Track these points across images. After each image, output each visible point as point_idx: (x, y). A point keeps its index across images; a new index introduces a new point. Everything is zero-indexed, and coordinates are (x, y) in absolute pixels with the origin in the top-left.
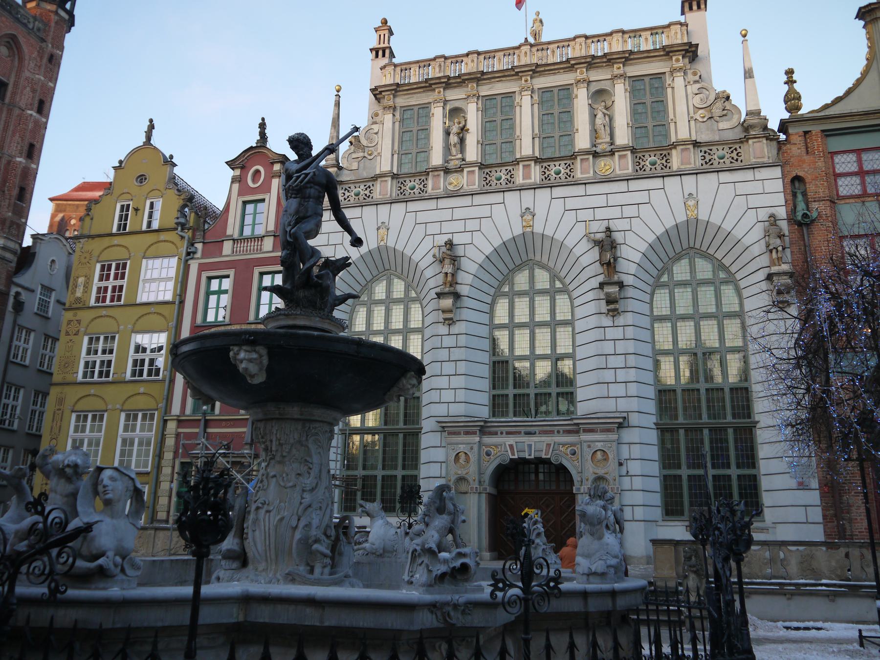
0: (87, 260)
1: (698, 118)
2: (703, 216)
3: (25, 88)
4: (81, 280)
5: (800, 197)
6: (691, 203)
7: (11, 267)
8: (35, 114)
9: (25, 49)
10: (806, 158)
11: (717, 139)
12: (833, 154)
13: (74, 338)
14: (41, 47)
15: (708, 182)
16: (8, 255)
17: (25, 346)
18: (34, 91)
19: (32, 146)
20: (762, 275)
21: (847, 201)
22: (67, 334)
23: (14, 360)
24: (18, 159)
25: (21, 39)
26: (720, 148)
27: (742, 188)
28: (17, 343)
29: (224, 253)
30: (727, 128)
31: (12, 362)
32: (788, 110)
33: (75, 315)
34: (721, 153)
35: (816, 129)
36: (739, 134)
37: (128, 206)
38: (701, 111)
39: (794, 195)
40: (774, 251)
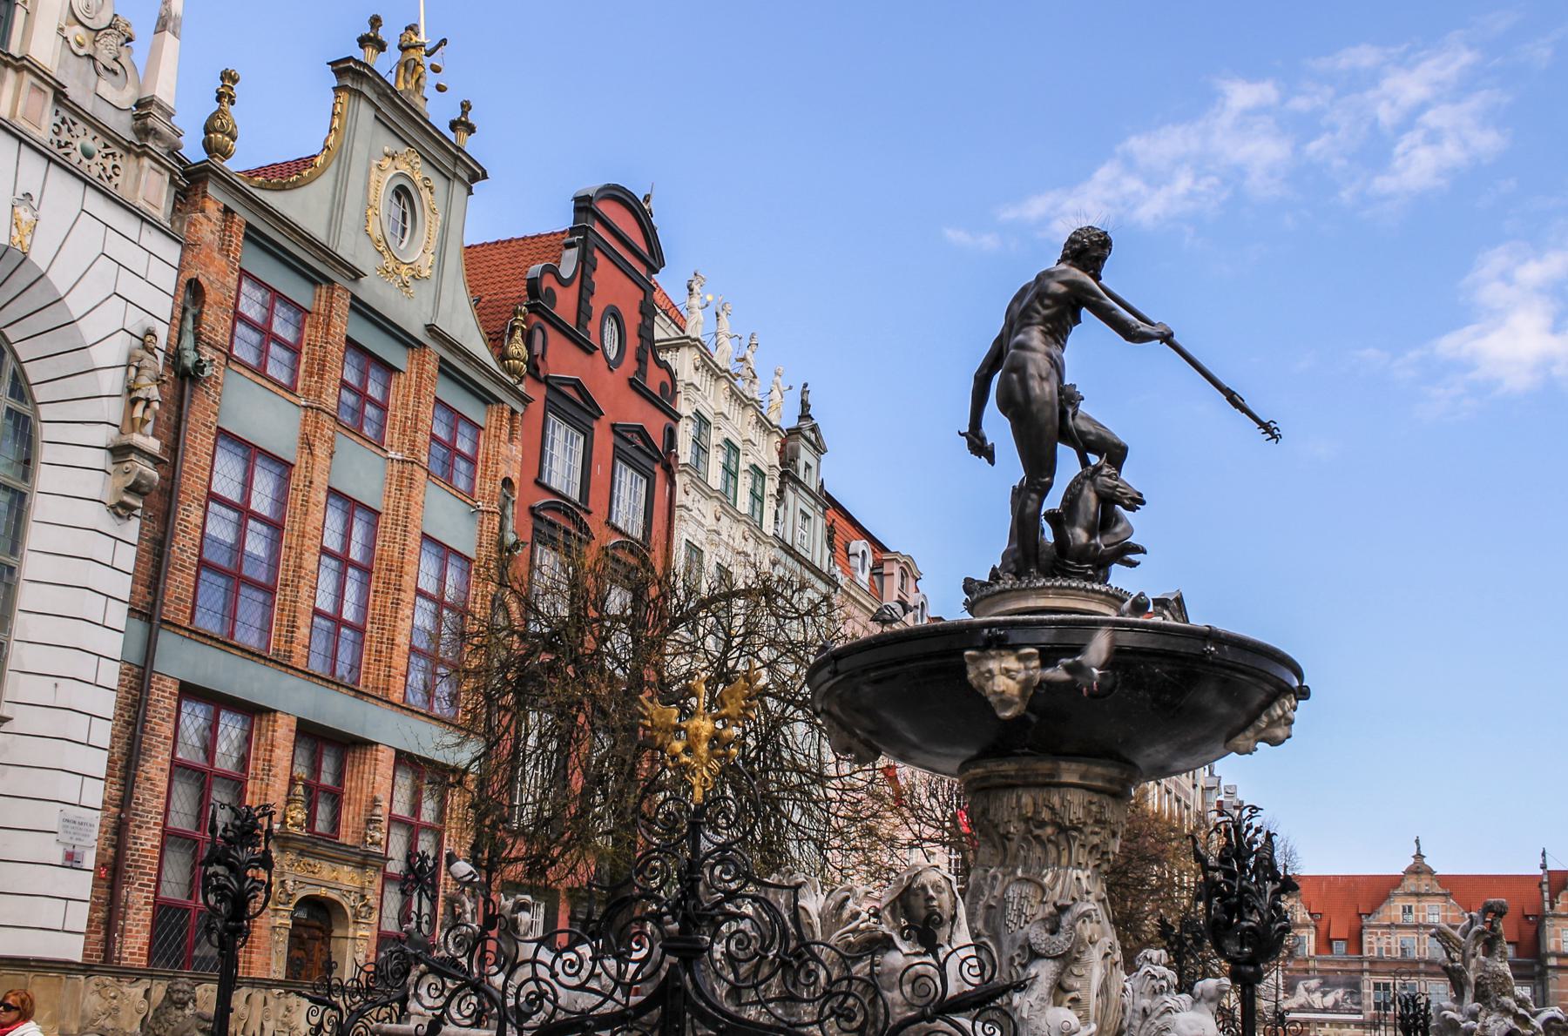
1: (71, 39)
2: (39, 257)
5: (189, 325)
6: (25, 215)
10: (216, 255)
11: (88, 104)
12: (244, 274)
15: (63, 193)
20: (105, 436)
21: (242, 370)
26: (91, 133)
27: (117, 247)
30: (111, 100)
32: (208, 146)
34: (90, 145)
35: (243, 214)
36: (122, 125)
38: (78, 29)
39: (185, 310)
40: (140, 407)
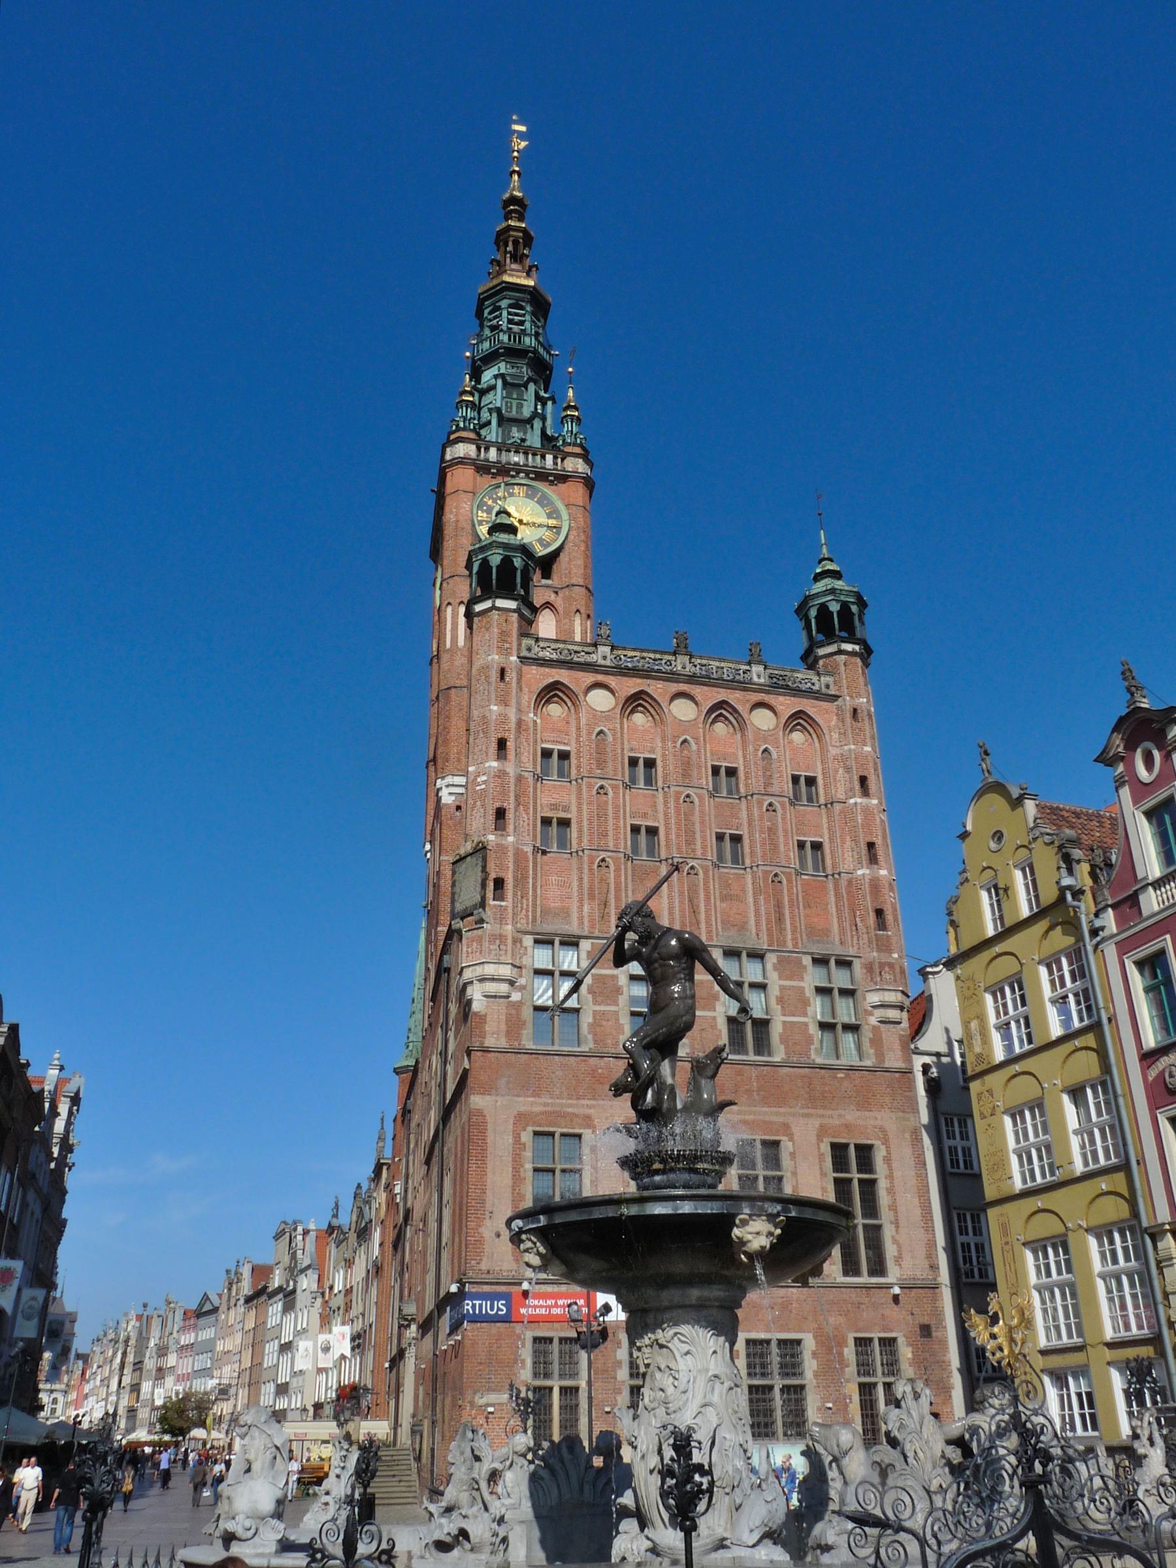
0: (972, 991)
3: (837, 771)
4: (974, 1025)
7: (902, 1030)
8: (859, 800)
9: (821, 722)
13: (990, 1120)
14: (838, 708)
16: (893, 1014)
17: (965, 1143)
18: (848, 769)
19: (871, 846)
22: (983, 1117)
23: (955, 1170)
24: (860, 872)
25: (811, 711)
28: (951, 1143)
29: (1145, 913)
31: (951, 1173)
33: (983, 1084)
37: (996, 887)
